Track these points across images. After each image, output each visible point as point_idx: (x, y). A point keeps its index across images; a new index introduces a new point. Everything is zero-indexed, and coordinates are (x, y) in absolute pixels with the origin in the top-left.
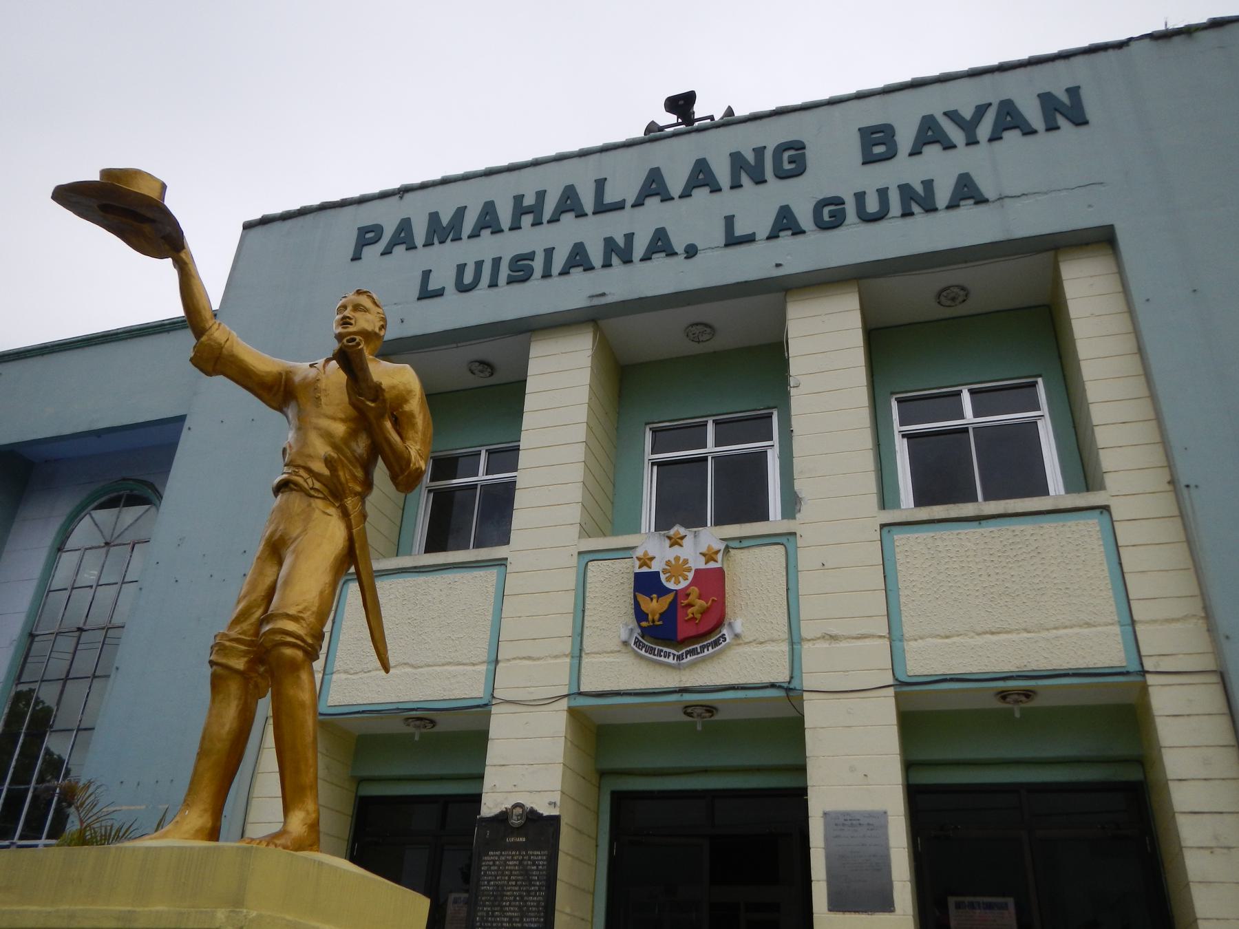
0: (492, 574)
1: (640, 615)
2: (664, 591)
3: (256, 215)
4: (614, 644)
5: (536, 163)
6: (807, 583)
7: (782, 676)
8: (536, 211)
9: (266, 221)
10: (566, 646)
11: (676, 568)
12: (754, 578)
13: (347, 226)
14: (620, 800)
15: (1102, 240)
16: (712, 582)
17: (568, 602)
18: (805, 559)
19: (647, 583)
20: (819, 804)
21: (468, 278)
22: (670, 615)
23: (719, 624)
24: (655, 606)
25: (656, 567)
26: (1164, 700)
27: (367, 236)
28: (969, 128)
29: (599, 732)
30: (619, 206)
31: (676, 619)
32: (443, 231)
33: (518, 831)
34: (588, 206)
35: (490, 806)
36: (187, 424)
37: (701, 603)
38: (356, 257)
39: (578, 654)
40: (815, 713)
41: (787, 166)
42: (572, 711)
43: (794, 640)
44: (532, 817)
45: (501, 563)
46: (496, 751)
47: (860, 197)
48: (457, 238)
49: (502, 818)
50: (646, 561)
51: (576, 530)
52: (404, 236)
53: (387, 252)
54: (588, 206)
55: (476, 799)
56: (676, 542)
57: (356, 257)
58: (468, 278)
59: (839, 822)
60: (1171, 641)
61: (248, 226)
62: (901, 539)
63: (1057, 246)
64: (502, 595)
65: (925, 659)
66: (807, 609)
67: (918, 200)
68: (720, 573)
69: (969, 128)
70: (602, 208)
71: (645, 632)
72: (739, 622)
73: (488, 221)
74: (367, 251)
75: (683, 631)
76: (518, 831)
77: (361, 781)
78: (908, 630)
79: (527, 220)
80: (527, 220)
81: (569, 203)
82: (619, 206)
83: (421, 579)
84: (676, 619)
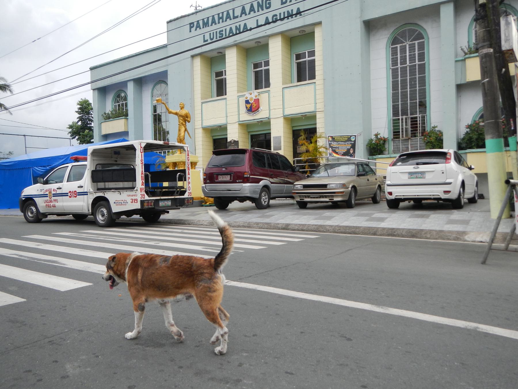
0: (225, 100)
1: (247, 108)
2: (249, 103)
3: (169, 20)
4: (244, 112)
5: (221, 4)
6: (271, 99)
7: (268, 116)
8: (222, 18)
9: (170, 21)
10: (237, 113)
11: (251, 99)
12: (264, 98)
14: (252, 137)
16: (257, 101)
17: (236, 105)
18: (271, 95)
19: (247, 102)
20: (272, 136)
21: (212, 37)
22: (251, 107)
23: (259, 108)
24: (249, 106)
25: (248, 99)
26: (318, 116)
27: (191, 25)
29: (245, 126)
30: (237, 17)
31: (252, 107)
32: (206, 24)
33: (233, 143)
34: (232, 17)
35: (229, 140)
36: (169, 73)
37: (255, 105)
38: (190, 31)
39: (239, 115)
40: (272, 122)
41: (268, 6)
42: (239, 124)
44: (235, 141)
45: (226, 99)
46: (229, 131)
47: (280, 14)
48: (208, 26)
49: (231, 142)
50: (246, 98)
51: (236, 92)
53: (196, 30)
54: (232, 17)
55: (227, 138)
56: (251, 94)
57: (190, 31)
58: (212, 37)
59: (275, 138)
60: (320, 106)
61: (168, 23)
64: (226, 105)
66: (271, 105)
67: (290, 15)
68: (258, 99)
70: (235, 18)
71: (248, 110)
72: (261, 108)
73: (214, 22)
75: (253, 110)
76: (233, 143)
77: (213, 136)
78: (286, 107)
79: (221, 20)
82: (237, 17)
83: (214, 102)
84: (252, 107)
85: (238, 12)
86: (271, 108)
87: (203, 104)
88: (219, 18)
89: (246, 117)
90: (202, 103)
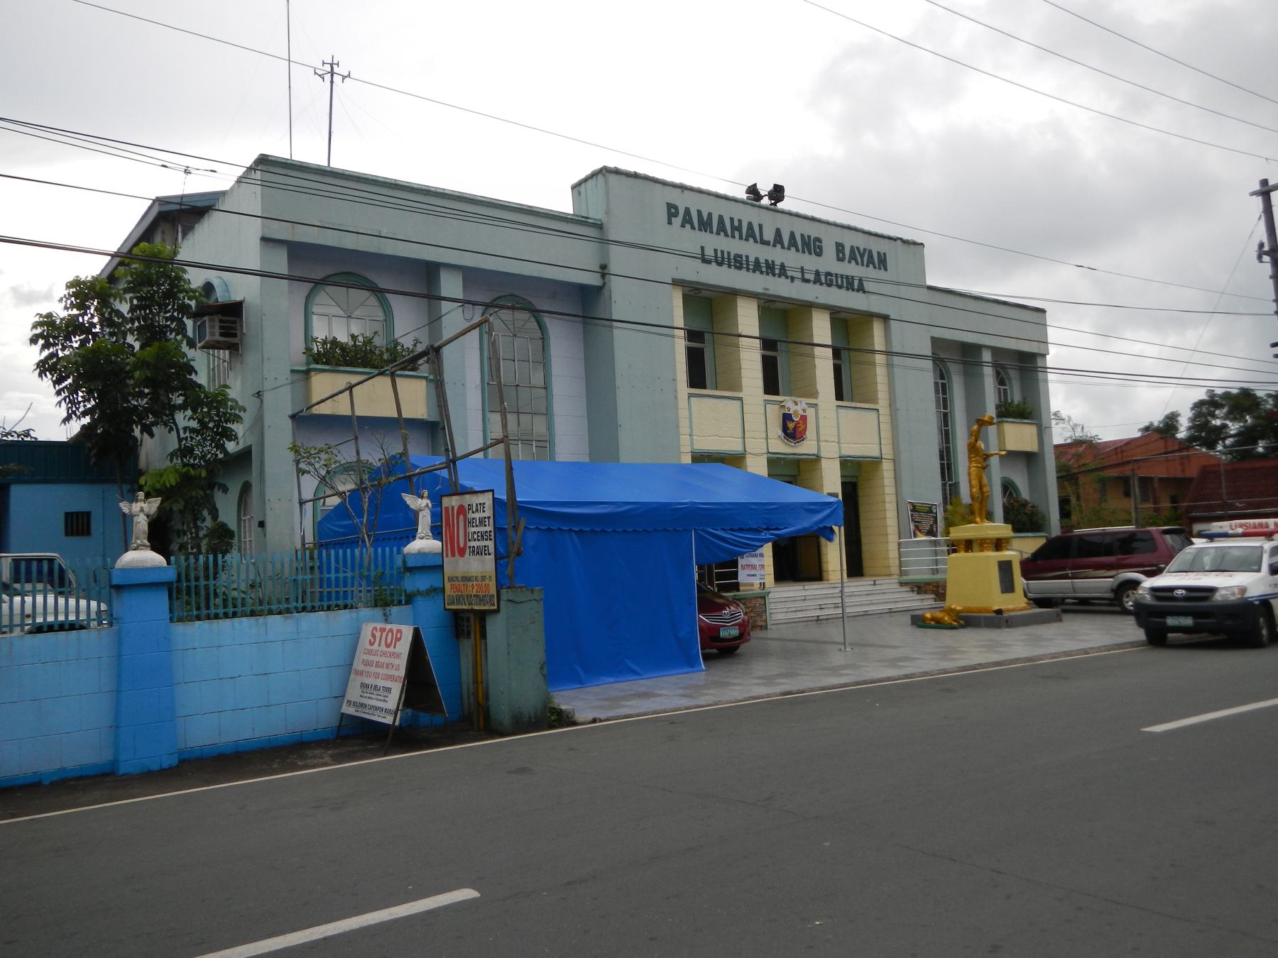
8: (739, 229)
13: (661, 198)
15: (885, 318)
16: (804, 418)
18: (821, 415)
19: (787, 418)
28: (862, 256)
30: (767, 243)
31: (792, 429)
32: (705, 225)
38: (670, 223)
43: (818, 440)
52: (687, 220)
57: (670, 223)
60: (887, 452)
62: (842, 411)
63: (871, 316)
65: (845, 452)
69: (862, 256)
73: (721, 228)
74: (673, 219)
80: (737, 234)
81: (751, 234)
85: (769, 235)
86: (822, 438)
87: (693, 399)
88: (734, 228)
89: (780, 446)
90: (690, 395)
